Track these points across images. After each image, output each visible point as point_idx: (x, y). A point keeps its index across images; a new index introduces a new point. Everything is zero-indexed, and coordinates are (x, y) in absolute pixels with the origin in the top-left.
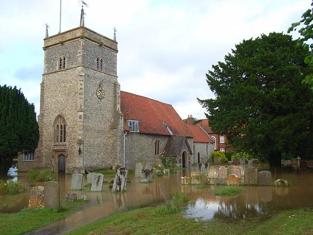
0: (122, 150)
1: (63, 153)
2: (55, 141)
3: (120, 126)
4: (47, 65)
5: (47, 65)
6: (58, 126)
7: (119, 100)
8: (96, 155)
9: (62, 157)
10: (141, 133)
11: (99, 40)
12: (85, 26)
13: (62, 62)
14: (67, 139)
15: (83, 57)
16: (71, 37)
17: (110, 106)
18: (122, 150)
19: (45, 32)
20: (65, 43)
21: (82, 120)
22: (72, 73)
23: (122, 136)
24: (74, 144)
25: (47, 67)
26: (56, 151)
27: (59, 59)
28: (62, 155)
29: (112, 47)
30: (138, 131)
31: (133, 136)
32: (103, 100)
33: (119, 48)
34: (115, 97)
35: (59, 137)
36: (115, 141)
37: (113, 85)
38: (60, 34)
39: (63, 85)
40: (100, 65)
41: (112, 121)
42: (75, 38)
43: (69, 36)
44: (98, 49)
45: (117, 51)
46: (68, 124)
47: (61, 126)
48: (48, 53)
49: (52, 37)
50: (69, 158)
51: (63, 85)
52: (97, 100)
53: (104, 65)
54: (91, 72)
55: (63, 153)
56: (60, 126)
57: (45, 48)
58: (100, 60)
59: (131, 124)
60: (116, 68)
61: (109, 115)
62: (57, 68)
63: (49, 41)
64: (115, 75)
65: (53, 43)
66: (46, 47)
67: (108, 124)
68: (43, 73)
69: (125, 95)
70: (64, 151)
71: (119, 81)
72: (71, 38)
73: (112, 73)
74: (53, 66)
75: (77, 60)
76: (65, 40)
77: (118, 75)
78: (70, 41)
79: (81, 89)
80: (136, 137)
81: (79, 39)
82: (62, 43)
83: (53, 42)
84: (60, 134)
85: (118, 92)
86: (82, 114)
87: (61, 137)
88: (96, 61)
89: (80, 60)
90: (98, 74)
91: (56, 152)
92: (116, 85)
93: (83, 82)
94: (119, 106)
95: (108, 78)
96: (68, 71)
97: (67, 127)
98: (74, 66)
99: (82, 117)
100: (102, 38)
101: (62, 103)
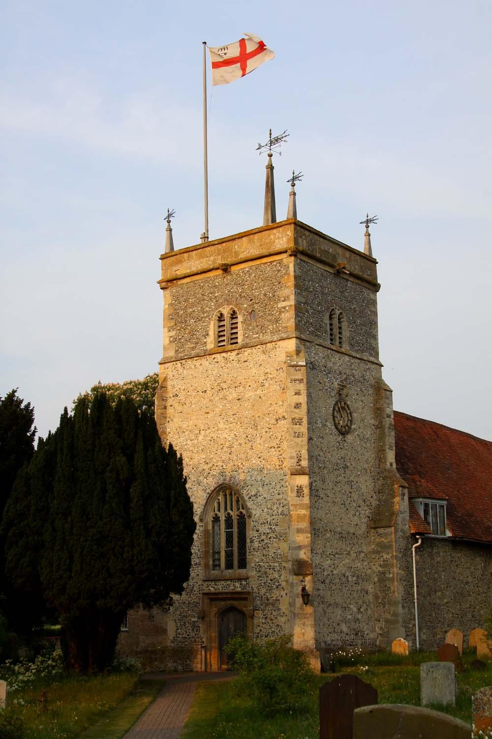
0: (409, 594)
1: (235, 603)
2: (206, 566)
3: (400, 519)
4: (173, 333)
5: (173, 333)
6: (216, 519)
7: (391, 439)
8: (339, 612)
9: (231, 616)
10: (455, 543)
11: (334, 257)
12: (300, 218)
13: (227, 322)
14: (254, 558)
15: (299, 310)
16: (255, 252)
17: (367, 455)
18: (409, 594)
19: (165, 235)
20: (233, 268)
21: (306, 500)
22: (263, 357)
23: (406, 552)
24: (276, 575)
25: (173, 340)
26: (213, 597)
27: (215, 317)
28: (232, 609)
29: (365, 276)
30: (449, 534)
31: (435, 551)
32: (350, 438)
33: (382, 277)
34: (380, 427)
35: (223, 554)
36: (386, 565)
37: (371, 391)
38: (206, 244)
39: (233, 395)
40: (336, 331)
41: (374, 503)
42: (270, 255)
43: (247, 249)
44: (329, 283)
45: (376, 287)
46: (256, 512)
47: (229, 519)
48: (176, 298)
49: (188, 251)
50: (259, 614)
51: (233, 395)
52: (336, 438)
53: (346, 333)
54: (319, 355)
55: (235, 603)
56: (223, 518)
57: (167, 283)
58: (336, 317)
59: (426, 512)
60: (375, 337)
61: (366, 485)
62: (210, 342)
63: (180, 262)
64: (372, 359)
65: (194, 269)
66: (171, 281)
67: (366, 511)
68: (160, 358)
69: (400, 417)
70: (243, 596)
71: (388, 376)
72: (256, 252)
73: (366, 356)
74: (196, 338)
75: (277, 321)
76: (234, 260)
77: (382, 359)
78: (250, 264)
79: (298, 406)
80: (442, 554)
81: (284, 256)
82: (226, 269)
83: (194, 264)
84: (223, 544)
85: (388, 411)
86: (303, 481)
87: (229, 555)
88: (328, 322)
89: (289, 319)
90: (338, 362)
91: (212, 600)
92: (382, 392)
93: (302, 387)
94: (391, 456)
95: (358, 370)
96: (249, 351)
97: (250, 524)
98: (268, 338)
99: (306, 491)
100: (340, 251)
101: (231, 447)
